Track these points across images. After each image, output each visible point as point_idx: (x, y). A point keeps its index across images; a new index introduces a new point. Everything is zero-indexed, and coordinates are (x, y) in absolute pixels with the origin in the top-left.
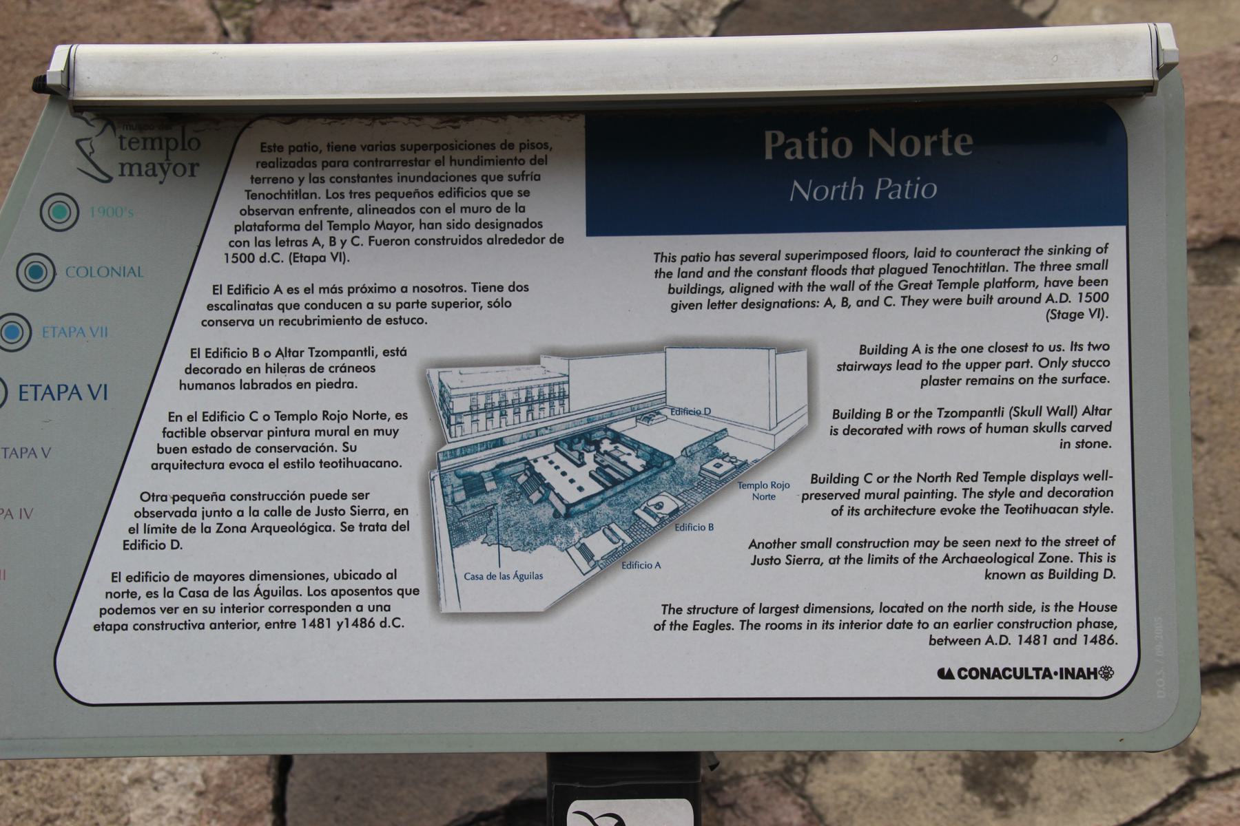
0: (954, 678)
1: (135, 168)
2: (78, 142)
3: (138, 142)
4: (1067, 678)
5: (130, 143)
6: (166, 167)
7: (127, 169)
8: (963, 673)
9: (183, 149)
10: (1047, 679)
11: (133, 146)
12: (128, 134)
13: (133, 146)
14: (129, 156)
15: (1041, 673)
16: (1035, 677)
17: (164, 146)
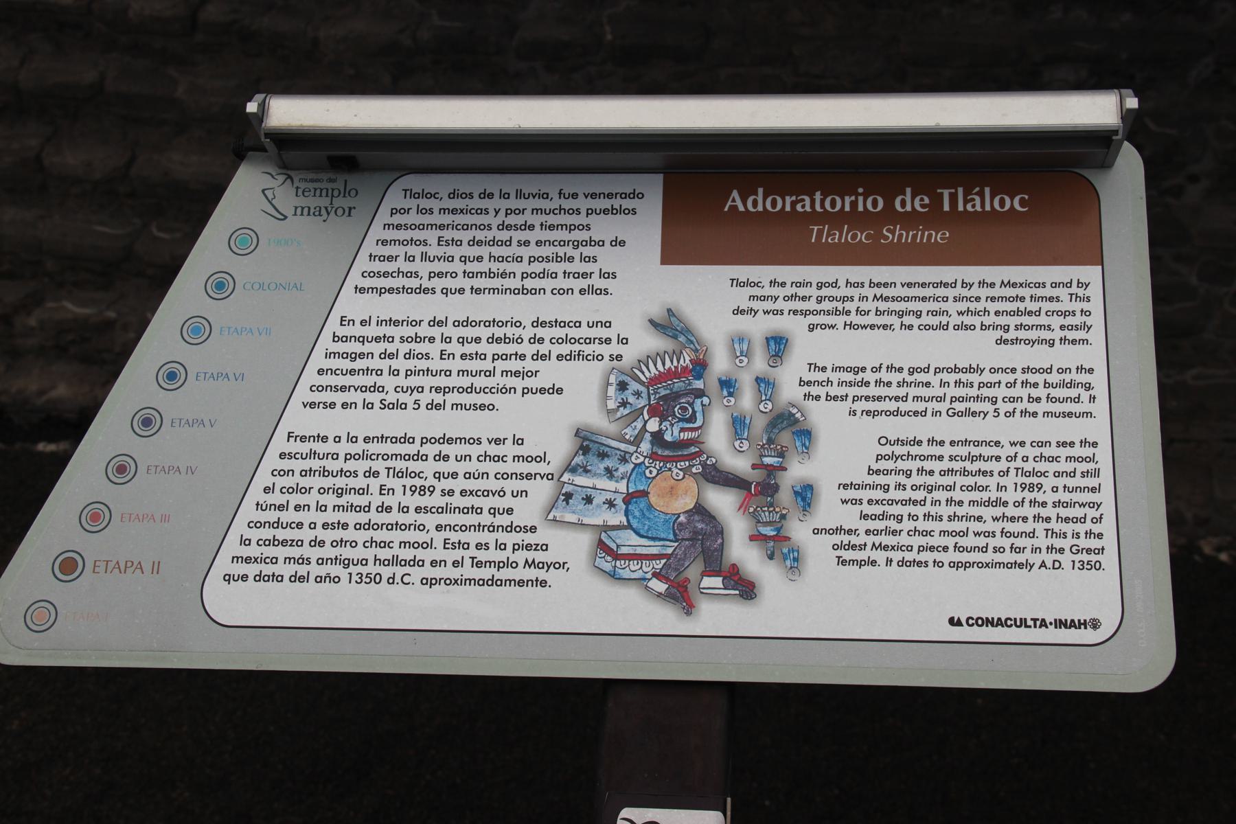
0: (962, 625)
1: (306, 210)
2: (263, 191)
3: (310, 191)
4: (1060, 628)
5: (304, 191)
6: (329, 209)
7: (300, 211)
8: (971, 622)
9: (344, 196)
10: (1044, 628)
11: (306, 194)
12: (303, 185)
13: (306, 194)
14: (301, 202)
15: (1038, 623)
16: (1033, 626)
17: (330, 194)
